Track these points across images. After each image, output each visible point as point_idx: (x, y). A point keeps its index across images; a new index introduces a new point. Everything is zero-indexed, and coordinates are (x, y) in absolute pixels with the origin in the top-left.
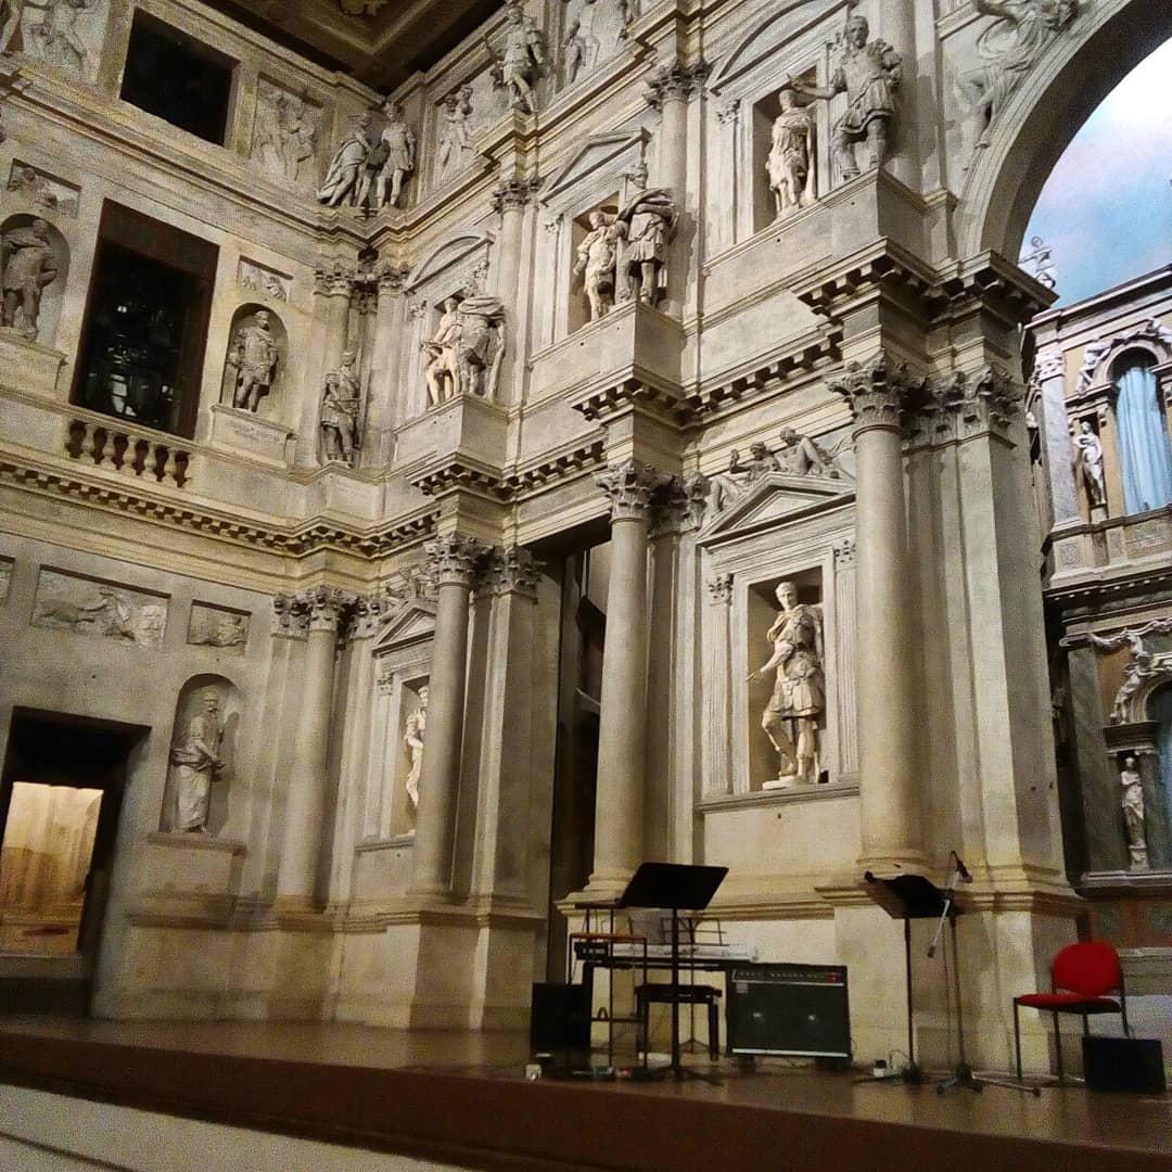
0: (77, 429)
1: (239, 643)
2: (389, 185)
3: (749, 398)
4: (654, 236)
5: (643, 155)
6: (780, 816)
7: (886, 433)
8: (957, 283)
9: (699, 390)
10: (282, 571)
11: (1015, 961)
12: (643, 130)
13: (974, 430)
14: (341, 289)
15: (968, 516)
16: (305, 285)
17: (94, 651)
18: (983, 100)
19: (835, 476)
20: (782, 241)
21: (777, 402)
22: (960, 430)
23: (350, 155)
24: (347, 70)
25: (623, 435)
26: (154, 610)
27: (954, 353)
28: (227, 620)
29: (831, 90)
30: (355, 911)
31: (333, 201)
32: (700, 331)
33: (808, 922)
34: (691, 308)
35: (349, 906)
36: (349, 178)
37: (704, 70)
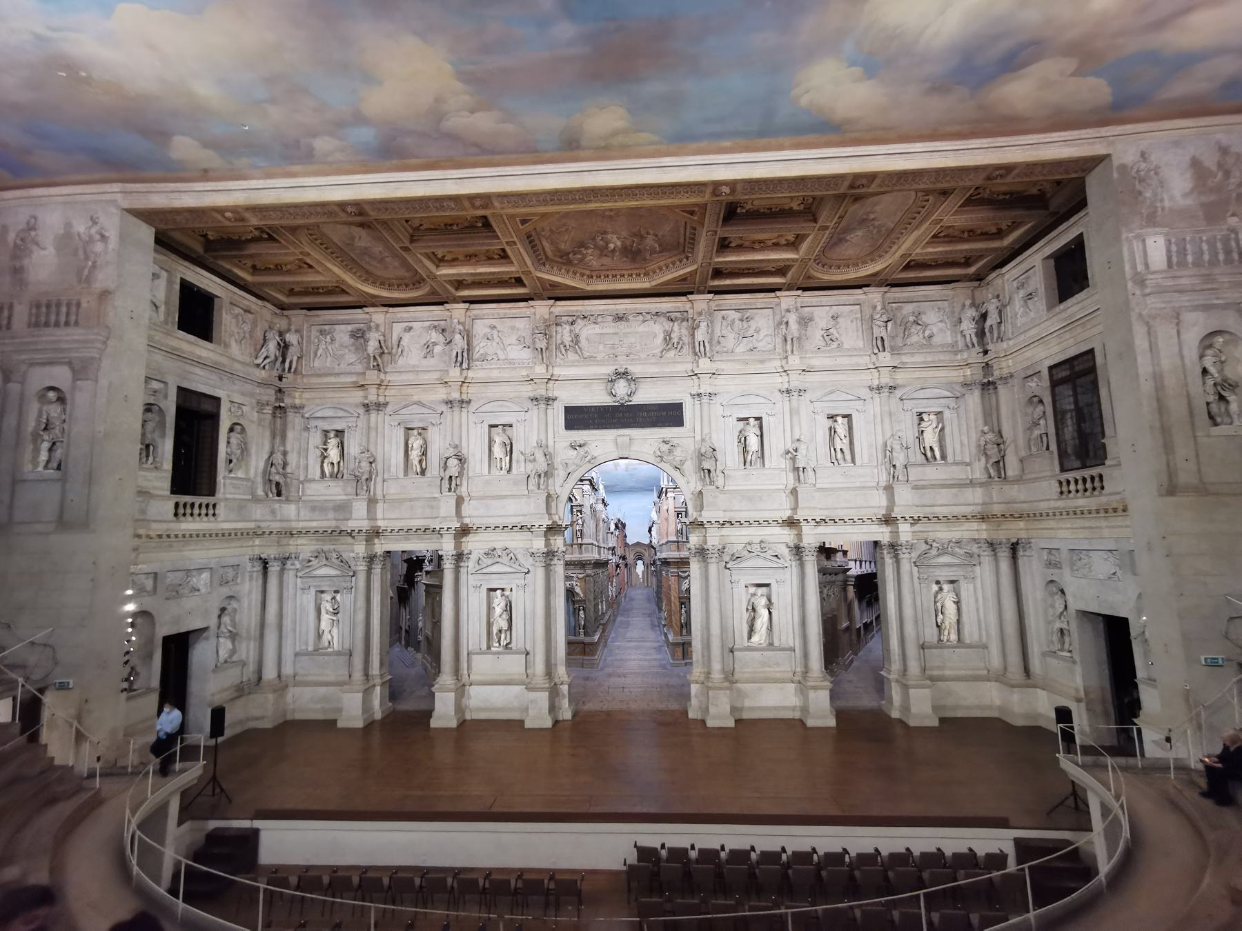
0: (177, 505)
1: (236, 577)
2: (291, 362)
10: (251, 543)
11: (564, 695)
14: (268, 410)
16: (253, 408)
17: (190, 602)
22: (555, 561)
23: (272, 347)
24: (268, 301)
26: (205, 576)
28: (230, 570)
30: (297, 678)
31: (262, 365)
35: (294, 677)
36: (272, 357)
37: (469, 402)
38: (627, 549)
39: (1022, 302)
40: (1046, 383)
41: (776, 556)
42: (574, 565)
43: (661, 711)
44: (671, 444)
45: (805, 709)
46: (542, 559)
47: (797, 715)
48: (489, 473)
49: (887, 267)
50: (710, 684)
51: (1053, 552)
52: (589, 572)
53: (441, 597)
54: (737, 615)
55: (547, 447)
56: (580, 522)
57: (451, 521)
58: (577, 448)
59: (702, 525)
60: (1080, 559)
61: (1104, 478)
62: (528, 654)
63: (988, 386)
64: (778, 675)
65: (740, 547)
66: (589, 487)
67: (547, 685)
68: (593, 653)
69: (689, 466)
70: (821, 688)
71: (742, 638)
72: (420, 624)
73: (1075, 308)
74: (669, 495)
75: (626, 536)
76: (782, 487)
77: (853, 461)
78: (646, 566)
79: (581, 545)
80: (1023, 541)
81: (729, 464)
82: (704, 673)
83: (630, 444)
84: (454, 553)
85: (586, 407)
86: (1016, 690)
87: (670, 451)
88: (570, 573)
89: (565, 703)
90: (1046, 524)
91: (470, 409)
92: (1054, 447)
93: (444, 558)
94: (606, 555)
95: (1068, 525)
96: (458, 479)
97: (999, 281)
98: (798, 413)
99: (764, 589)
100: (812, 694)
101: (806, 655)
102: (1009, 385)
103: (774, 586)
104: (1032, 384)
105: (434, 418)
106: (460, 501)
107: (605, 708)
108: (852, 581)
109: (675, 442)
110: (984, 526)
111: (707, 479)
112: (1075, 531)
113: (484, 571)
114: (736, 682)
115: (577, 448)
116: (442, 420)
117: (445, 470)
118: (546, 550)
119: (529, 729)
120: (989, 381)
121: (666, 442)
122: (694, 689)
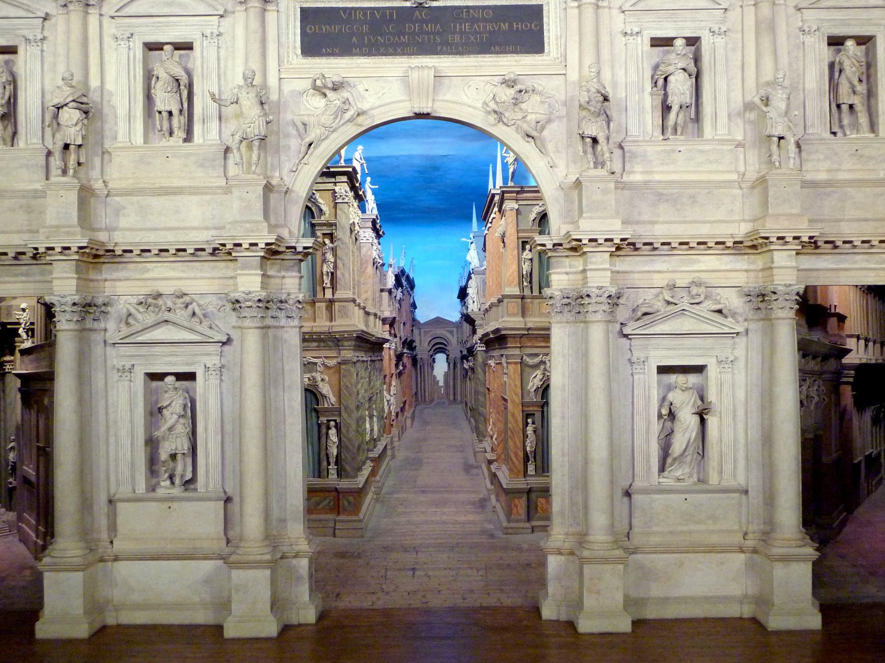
3: (147, 257)
4: (81, 129)
5: (43, 29)
6: (170, 508)
7: (258, 330)
8: (295, 248)
9: (114, 246)
11: (299, 579)
12: (47, 14)
13: (291, 323)
15: (287, 368)
18: (308, 140)
19: (210, 328)
20: (170, 159)
21: (166, 264)
25: (66, 272)
27: (283, 277)
29: (229, 103)
32: (108, 195)
33: (191, 562)
34: (95, 173)
38: (416, 332)
41: (720, 311)
42: (319, 340)
43: (487, 608)
44: (518, 87)
45: (763, 600)
46: (254, 312)
47: (747, 611)
48: (145, 143)
50: (586, 553)
52: (348, 354)
53: (52, 396)
54: (640, 425)
55: (264, 85)
56: (330, 257)
57: (68, 233)
58: (327, 92)
59: (576, 248)
62: (228, 500)
64: (714, 539)
65: (649, 295)
66: (348, 189)
67: (268, 557)
68: (356, 508)
69: (555, 133)
70: (797, 559)
71: (649, 468)
72: (12, 456)
74: (509, 205)
75: (414, 306)
76: (734, 177)
77: (873, 127)
78: (453, 364)
79: (331, 302)
81: (633, 130)
82: (573, 535)
83: (436, 89)
84: (77, 298)
85: (345, 9)
87: (516, 102)
88: (310, 357)
89: (303, 592)
91: (105, 10)
93: (57, 309)
94: (379, 330)
96: (83, 151)
98: (772, 28)
99: (692, 379)
100: (779, 571)
101: (770, 499)
103: (713, 371)
105: (33, 29)
106: (86, 195)
107: (379, 605)
108: (850, 376)
109: (528, 83)
111: (590, 156)
113: (140, 338)
114: (635, 551)
115: (327, 92)
116: (46, 34)
117: (54, 136)
118: (264, 294)
119: (233, 639)
121: (509, 83)
122: (553, 563)
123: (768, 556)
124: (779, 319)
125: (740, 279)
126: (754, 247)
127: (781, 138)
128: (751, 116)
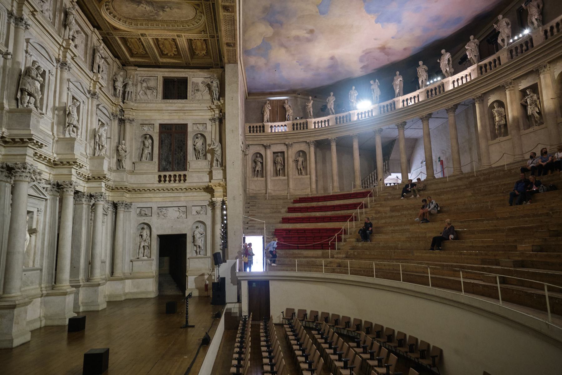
39: (144, 89)
40: (157, 129)
41: (44, 188)
47: (43, 324)
49: (128, 32)
50: (17, 302)
51: (144, 209)
60: (161, 212)
61: (187, 176)
63: (122, 121)
64: (33, 292)
73: (181, 105)
80: (129, 204)
86: (122, 281)
90: (146, 195)
92: (156, 159)
95: (161, 196)
97: (133, 72)
102: (131, 124)
104: (146, 128)
110: (111, 194)
112: (165, 198)
120: (121, 118)
123: (65, 294)
124: (69, 195)
125: (46, 176)
126: (56, 165)
127: (74, 126)
128: (56, 112)
